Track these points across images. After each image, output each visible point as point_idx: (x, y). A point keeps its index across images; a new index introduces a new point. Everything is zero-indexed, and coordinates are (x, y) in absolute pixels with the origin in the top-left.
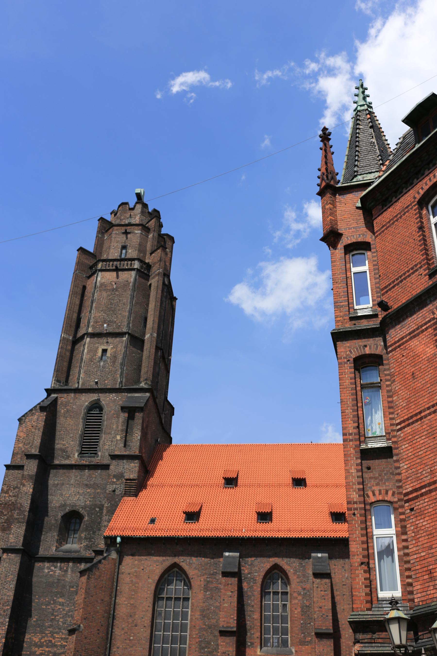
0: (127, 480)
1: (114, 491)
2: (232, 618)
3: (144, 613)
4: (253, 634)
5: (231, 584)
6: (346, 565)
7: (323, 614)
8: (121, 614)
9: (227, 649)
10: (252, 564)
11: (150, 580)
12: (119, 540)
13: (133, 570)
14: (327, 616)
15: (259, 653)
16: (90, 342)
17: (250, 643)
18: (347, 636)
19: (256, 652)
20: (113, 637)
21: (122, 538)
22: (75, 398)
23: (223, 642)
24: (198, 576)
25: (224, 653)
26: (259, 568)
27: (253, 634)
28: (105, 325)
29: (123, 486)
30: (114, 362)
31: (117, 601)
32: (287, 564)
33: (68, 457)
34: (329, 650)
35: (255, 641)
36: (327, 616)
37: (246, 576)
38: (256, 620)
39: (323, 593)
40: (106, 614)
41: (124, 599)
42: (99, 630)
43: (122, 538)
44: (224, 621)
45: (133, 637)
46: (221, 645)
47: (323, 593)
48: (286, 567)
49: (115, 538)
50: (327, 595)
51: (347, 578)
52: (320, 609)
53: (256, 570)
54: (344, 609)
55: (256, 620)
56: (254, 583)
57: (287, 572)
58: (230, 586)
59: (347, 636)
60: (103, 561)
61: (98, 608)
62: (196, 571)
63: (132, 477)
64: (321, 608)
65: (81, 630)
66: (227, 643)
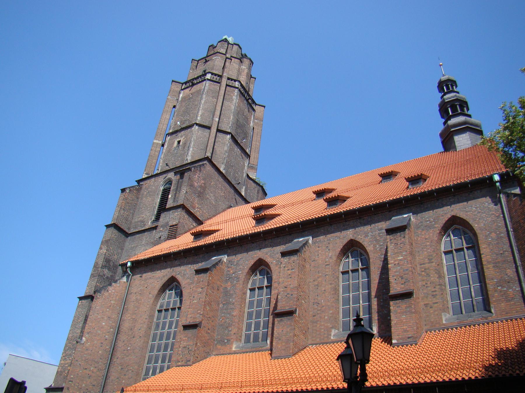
0: (171, 226)
1: (160, 238)
2: (198, 313)
3: (141, 325)
4: (231, 331)
5: (202, 281)
6: (331, 244)
7: (288, 294)
8: (124, 329)
9: (188, 343)
10: (237, 264)
11: (151, 295)
12: (129, 264)
13: (139, 289)
14: (292, 295)
15: (234, 349)
16: (170, 140)
17: (227, 340)
18: (326, 318)
19: (231, 348)
20: (115, 350)
21: (132, 262)
22: (155, 181)
23: (185, 337)
24: (189, 285)
25: (185, 347)
26: (243, 266)
27: (231, 331)
28: (178, 123)
29: (167, 232)
30: (184, 148)
31: (122, 318)
32: (270, 256)
33: (145, 225)
34: (288, 330)
35: (232, 337)
36: (292, 295)
37: (231, 276)
38: (235, 316)
39: (289, 272)
40: (112, 330)
41: (129, 315)
42: (102, 343)
43: (132, 262)
44: (191, 317)
45: (130, 347)
46: (183, 340)
47: (289, 272)
48: (268, 260)
49: (127, 264)
50: (295, 272)
51: (331, 258)
52: (285, 289)
53: (241, 268)
54: (325, 290)
55: (235, 316)
56: (237, 281)
57: (270, 264)
58: (201, 282)
59: (326, 318)
60: (113, 284)
61: (104, 324)
62: (188, 280)
63: (174, 223)
64: (286, 287)
65: (83, 342)
66: (189, 338)
